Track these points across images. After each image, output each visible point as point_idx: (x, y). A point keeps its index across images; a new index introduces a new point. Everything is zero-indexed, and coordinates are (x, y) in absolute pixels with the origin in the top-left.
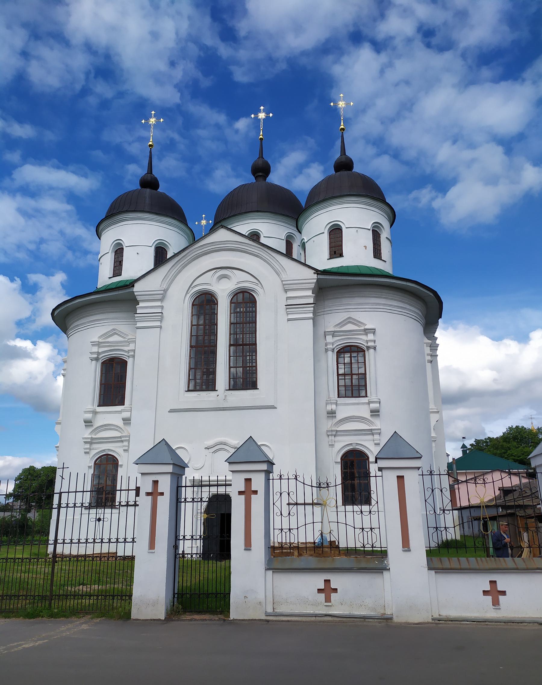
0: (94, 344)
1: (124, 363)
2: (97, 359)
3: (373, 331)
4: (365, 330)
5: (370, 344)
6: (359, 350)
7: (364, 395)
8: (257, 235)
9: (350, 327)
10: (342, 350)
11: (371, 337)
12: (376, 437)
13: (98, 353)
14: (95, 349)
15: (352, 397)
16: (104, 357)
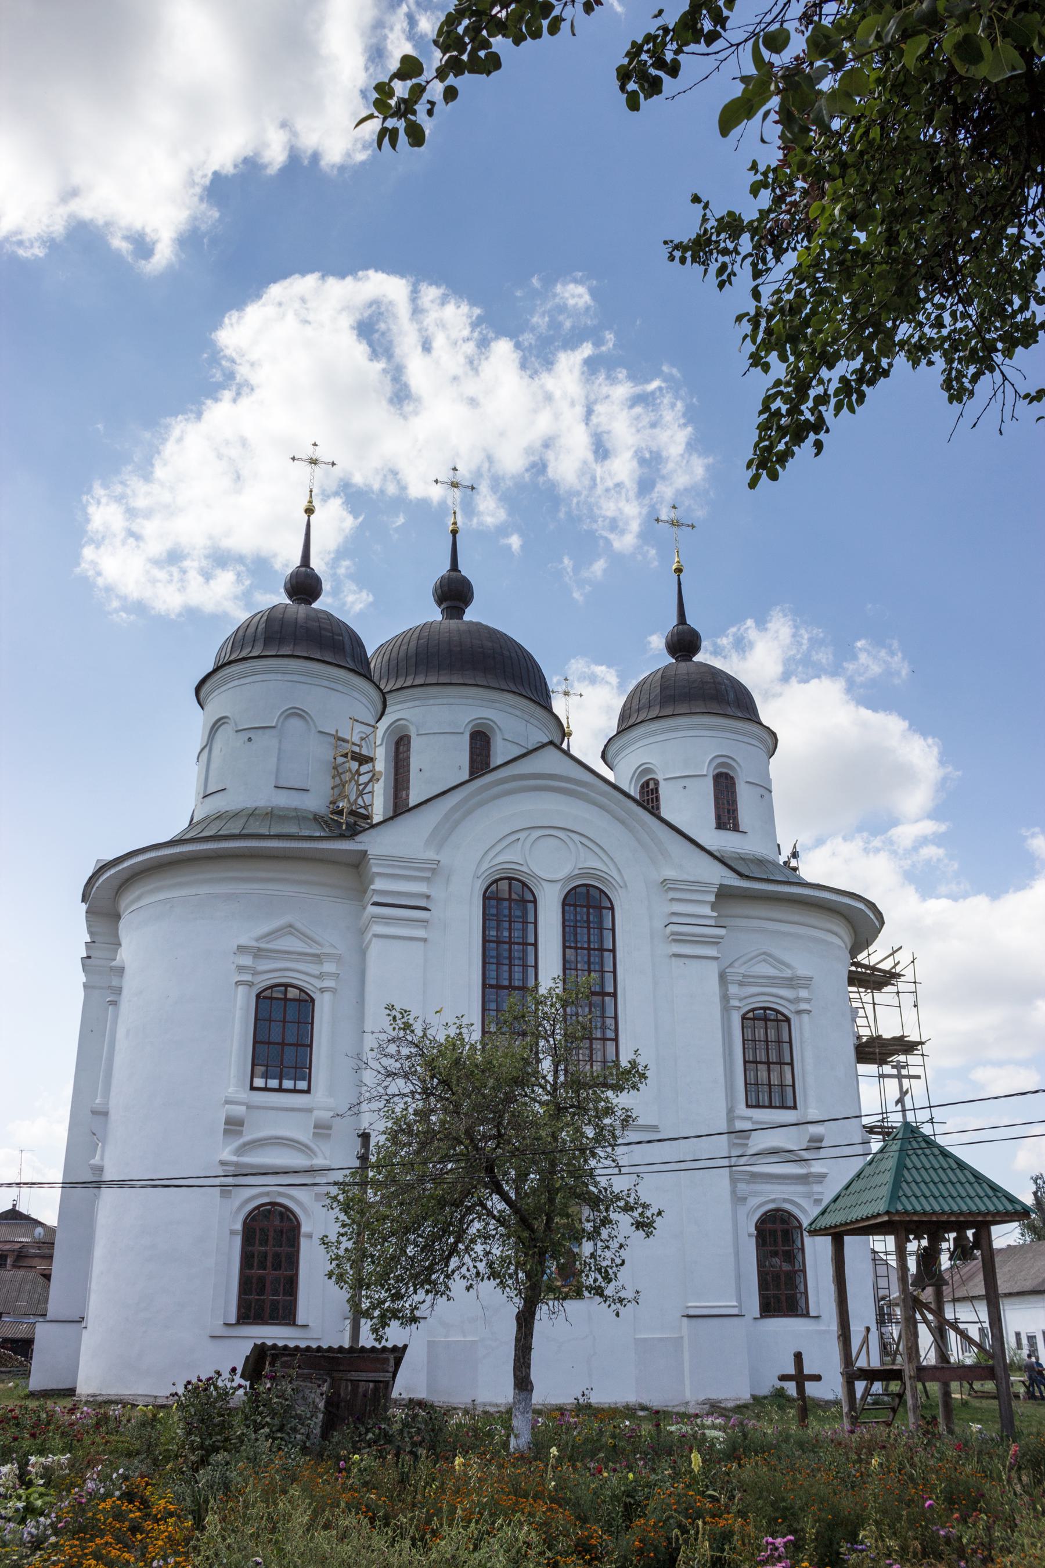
0: (241, 949)
1: (306, 1002)
2: (250, 984)
3: (805, 982)
4: (791, 979)
5: (804, 1006)
6: (780, 1017)
7: (790, 1103)
8: (484, 733)
9: (765, 969)
10: (750, 1015)
11: (803, 993)
12: (817, 1188)
13: (255, 973)
14: (247, 961)
15: (770, 1106)
16: (263, 981)
